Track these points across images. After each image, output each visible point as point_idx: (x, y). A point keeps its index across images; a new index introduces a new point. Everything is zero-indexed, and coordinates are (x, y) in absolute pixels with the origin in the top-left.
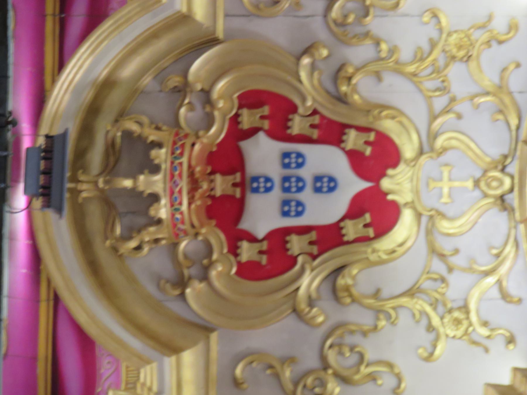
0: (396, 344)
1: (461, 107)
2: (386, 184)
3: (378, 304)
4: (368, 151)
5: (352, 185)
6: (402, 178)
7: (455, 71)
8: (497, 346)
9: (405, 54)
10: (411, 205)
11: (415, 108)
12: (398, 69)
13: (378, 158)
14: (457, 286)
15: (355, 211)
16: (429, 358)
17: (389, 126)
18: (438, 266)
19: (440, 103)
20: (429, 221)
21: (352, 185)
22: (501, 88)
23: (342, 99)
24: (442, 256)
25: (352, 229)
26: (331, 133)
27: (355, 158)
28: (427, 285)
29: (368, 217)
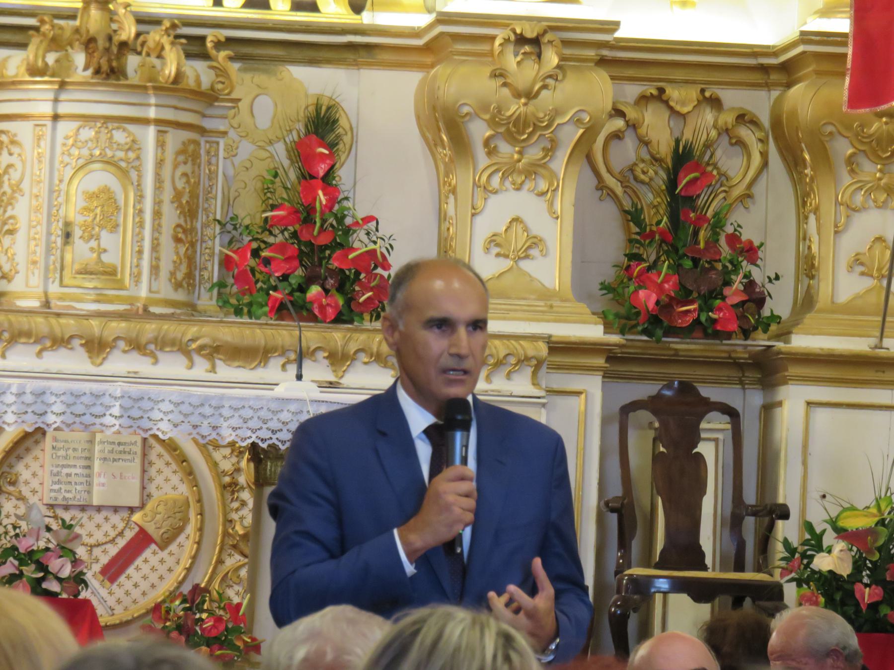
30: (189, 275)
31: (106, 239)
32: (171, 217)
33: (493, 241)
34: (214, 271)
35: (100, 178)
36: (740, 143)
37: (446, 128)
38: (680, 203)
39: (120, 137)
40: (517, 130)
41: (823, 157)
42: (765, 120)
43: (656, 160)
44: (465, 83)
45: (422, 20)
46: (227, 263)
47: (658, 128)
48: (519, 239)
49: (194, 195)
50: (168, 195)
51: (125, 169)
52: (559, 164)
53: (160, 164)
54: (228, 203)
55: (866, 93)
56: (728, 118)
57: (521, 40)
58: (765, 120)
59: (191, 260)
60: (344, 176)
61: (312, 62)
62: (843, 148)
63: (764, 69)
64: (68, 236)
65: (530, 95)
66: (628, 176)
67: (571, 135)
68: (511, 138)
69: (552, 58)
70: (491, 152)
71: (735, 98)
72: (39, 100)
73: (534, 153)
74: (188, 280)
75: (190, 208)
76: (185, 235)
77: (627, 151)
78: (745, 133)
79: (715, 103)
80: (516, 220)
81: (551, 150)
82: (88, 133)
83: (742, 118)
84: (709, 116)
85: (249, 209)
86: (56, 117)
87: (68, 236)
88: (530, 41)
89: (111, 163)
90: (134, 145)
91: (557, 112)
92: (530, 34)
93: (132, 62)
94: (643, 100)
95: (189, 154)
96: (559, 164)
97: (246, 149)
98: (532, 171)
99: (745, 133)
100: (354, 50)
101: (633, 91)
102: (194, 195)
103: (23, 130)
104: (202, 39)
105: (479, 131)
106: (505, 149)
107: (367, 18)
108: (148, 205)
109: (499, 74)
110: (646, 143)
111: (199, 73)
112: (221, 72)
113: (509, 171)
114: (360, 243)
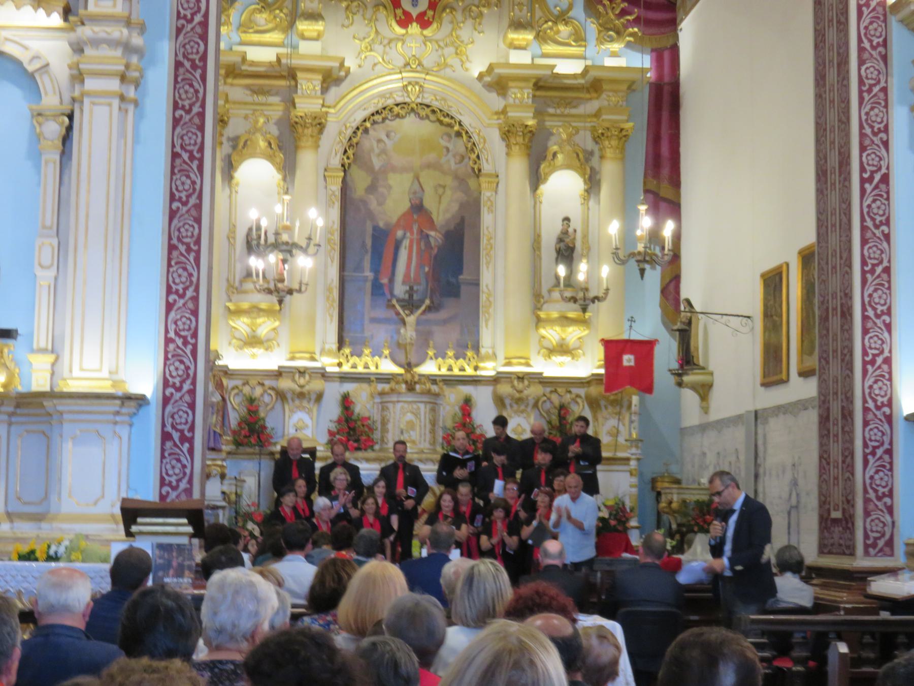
0: (360, 26)
1: (440, 52)
2: (415, 24)
3: (373, 20)
4: (426, 18)
5: (414, 13)
6: (391, 81)
7: (451, 50)
8: (358, 61)
9: (459, 32)
10: (407, 32)
11: (439, 36)
12: (453, 29)
13: (423, 21)
14: (379, 48)
15: (406, 13)
16: (354, 37)
17: (435, 25)
18: (386, 42)
19: (442, 44)
20: (402, 39)
21: (414, 13)
22: (446, 65)
23: (444, 10)
24: (389, 43)
25: (399, 12)
26: (433, 6)
27: (423, 14)
28: (380, 37)
29: (403, 17)
30: (434, 442)
31: (412, 433)
32: (428, 426)
33: (514, 430)
34: (440, 440)
35: (409, 417)
36: (577, 403)
37: (499, 401)
38: (562, 418)
39: (415, 406)
40: (519, 401)
41: (599, 406)
42: (583, 395)
43: (555, 407)
44: (505, 389)
45: (493, 373)
46: (444, 438)
47: (555, 398)
48: (520, 430)
49: (434, 420)
50: (428, 421)
51: (416, 414)
52: (529, 409)
53: (425, 413)
54: (444, 422)
55: (608, 389)
56: (573, 396)
57: (519, 378)
58: (583, 395)
59: (434, 438)
60: (474, 414)
61: (465, 384)
62: (603, 403)
63: (582, 383)
64: (402, 432)
65: (520, 392)
66: (548, 412)
67: (531, 402)
68: (517, 403)
69: (526, 382)
70: (511, 406)
71: (575, 391)
72: (394, 399)
73: (522, 407)
74: (433, 442)
75: (433, 423)
76: (433, 432)
77: (548, 405)
78: (579, 400)
79: (570, 392)
80: (519, 425)
81: (527, 406)
82: (406, 405)
83: (578, 396)
84: (568, 396)
85: (450, 424)
86: (398, 402)
87: (402, 432)
88: (521, 378)
89: (413, 413)
90: (419, 408)
91: (527, 397)
92: (521, 375)
93: (418, 387)
94: (551, 392)
95: (433, 410)
96: (529, 409)
97: (448, 408)
98: (522, 412)
99: (579, 400)
100: (475, 381)
101: (548, 389)
102: (434, 420)
103: (390, 406)
104: (435, 380)
105: (507, 402)
106: (515, 407)
107: (479, 373)
108: (423, 424)
109: (513, 387)
110: (551, 402)
111: (434, 388)
112: (441, 389)
113: (516, 412)
114: (478, 432)
